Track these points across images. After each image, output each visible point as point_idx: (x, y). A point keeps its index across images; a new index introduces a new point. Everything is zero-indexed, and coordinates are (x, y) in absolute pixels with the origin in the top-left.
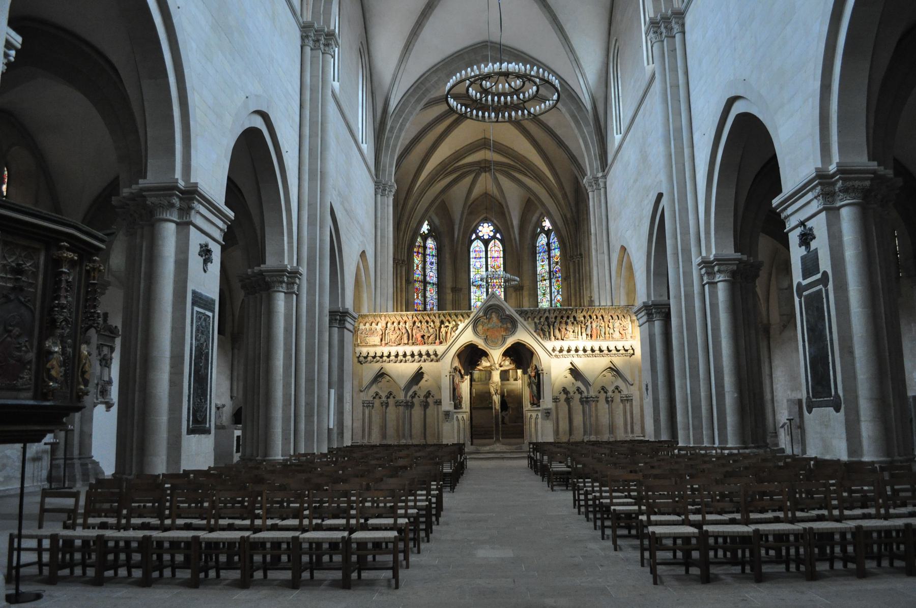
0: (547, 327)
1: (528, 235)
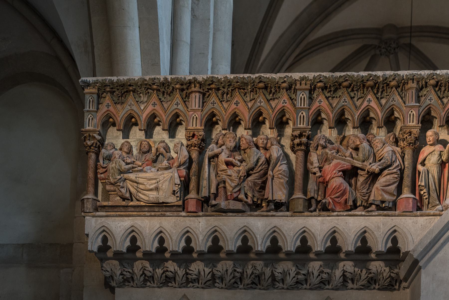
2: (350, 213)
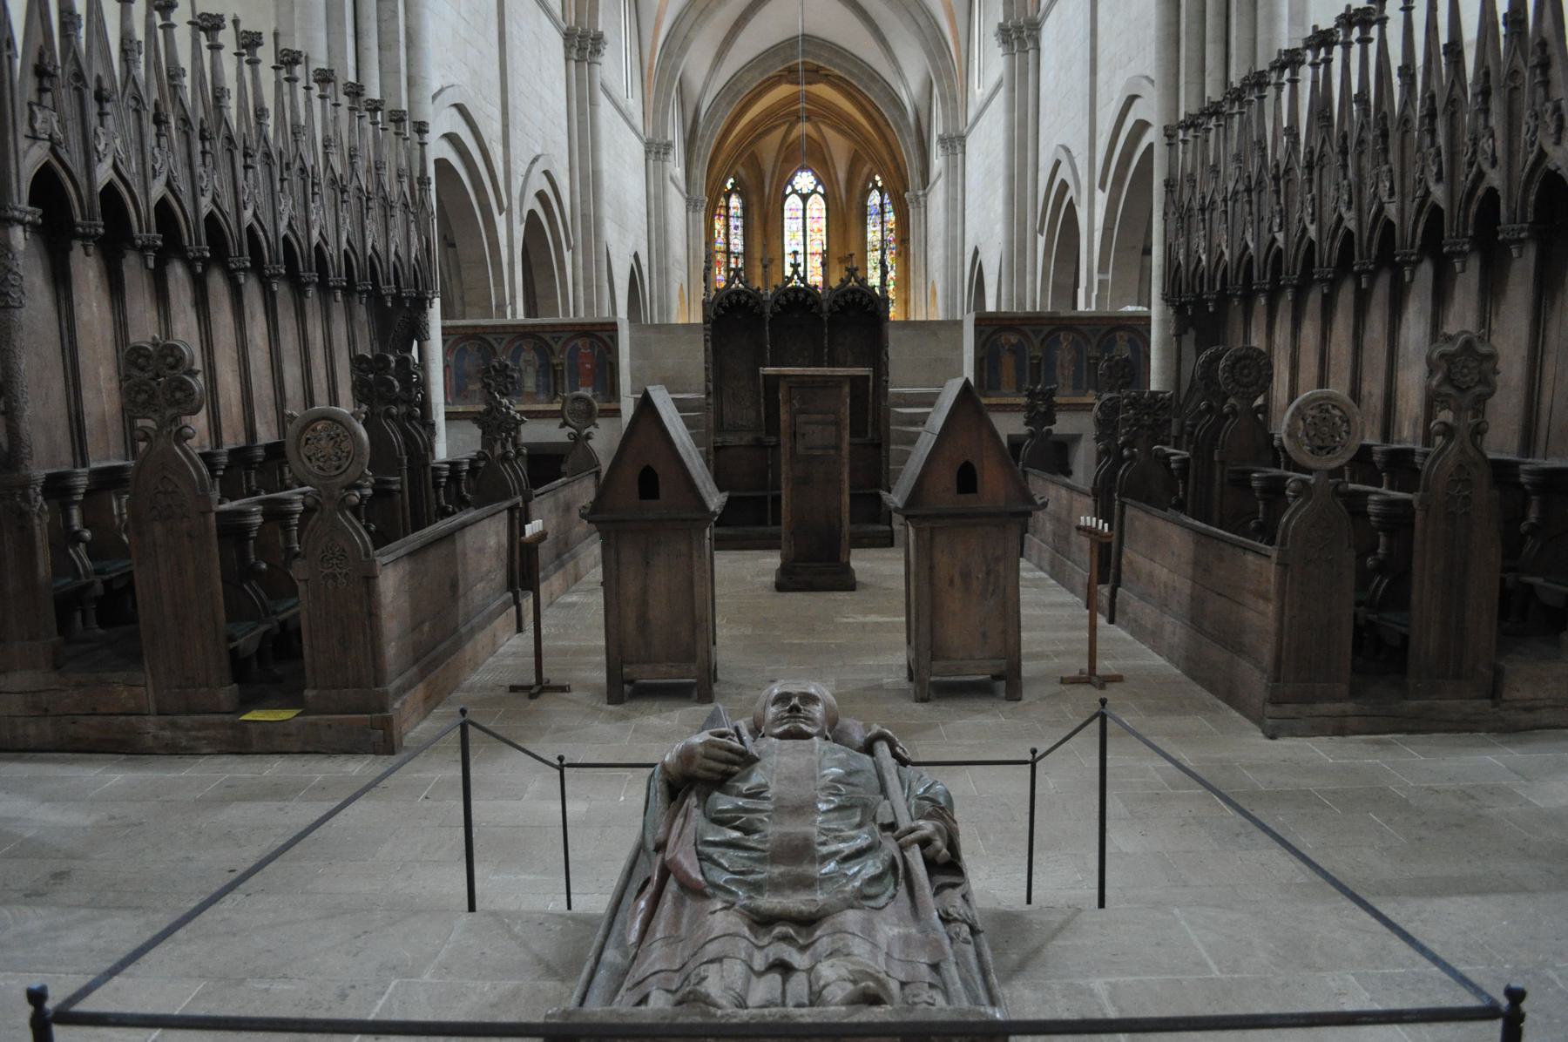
1: (857, 192)
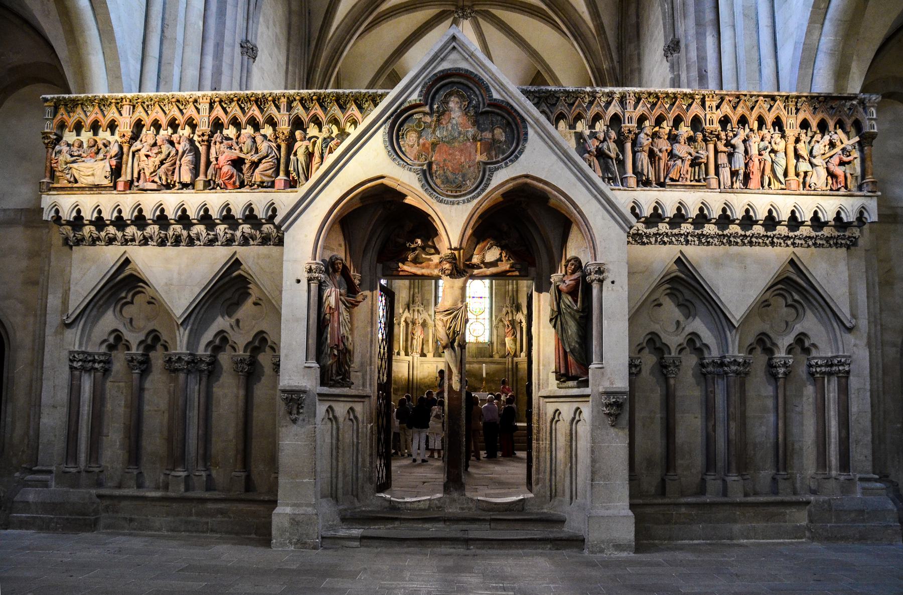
0: (613, 146)
2: (239, 190)
